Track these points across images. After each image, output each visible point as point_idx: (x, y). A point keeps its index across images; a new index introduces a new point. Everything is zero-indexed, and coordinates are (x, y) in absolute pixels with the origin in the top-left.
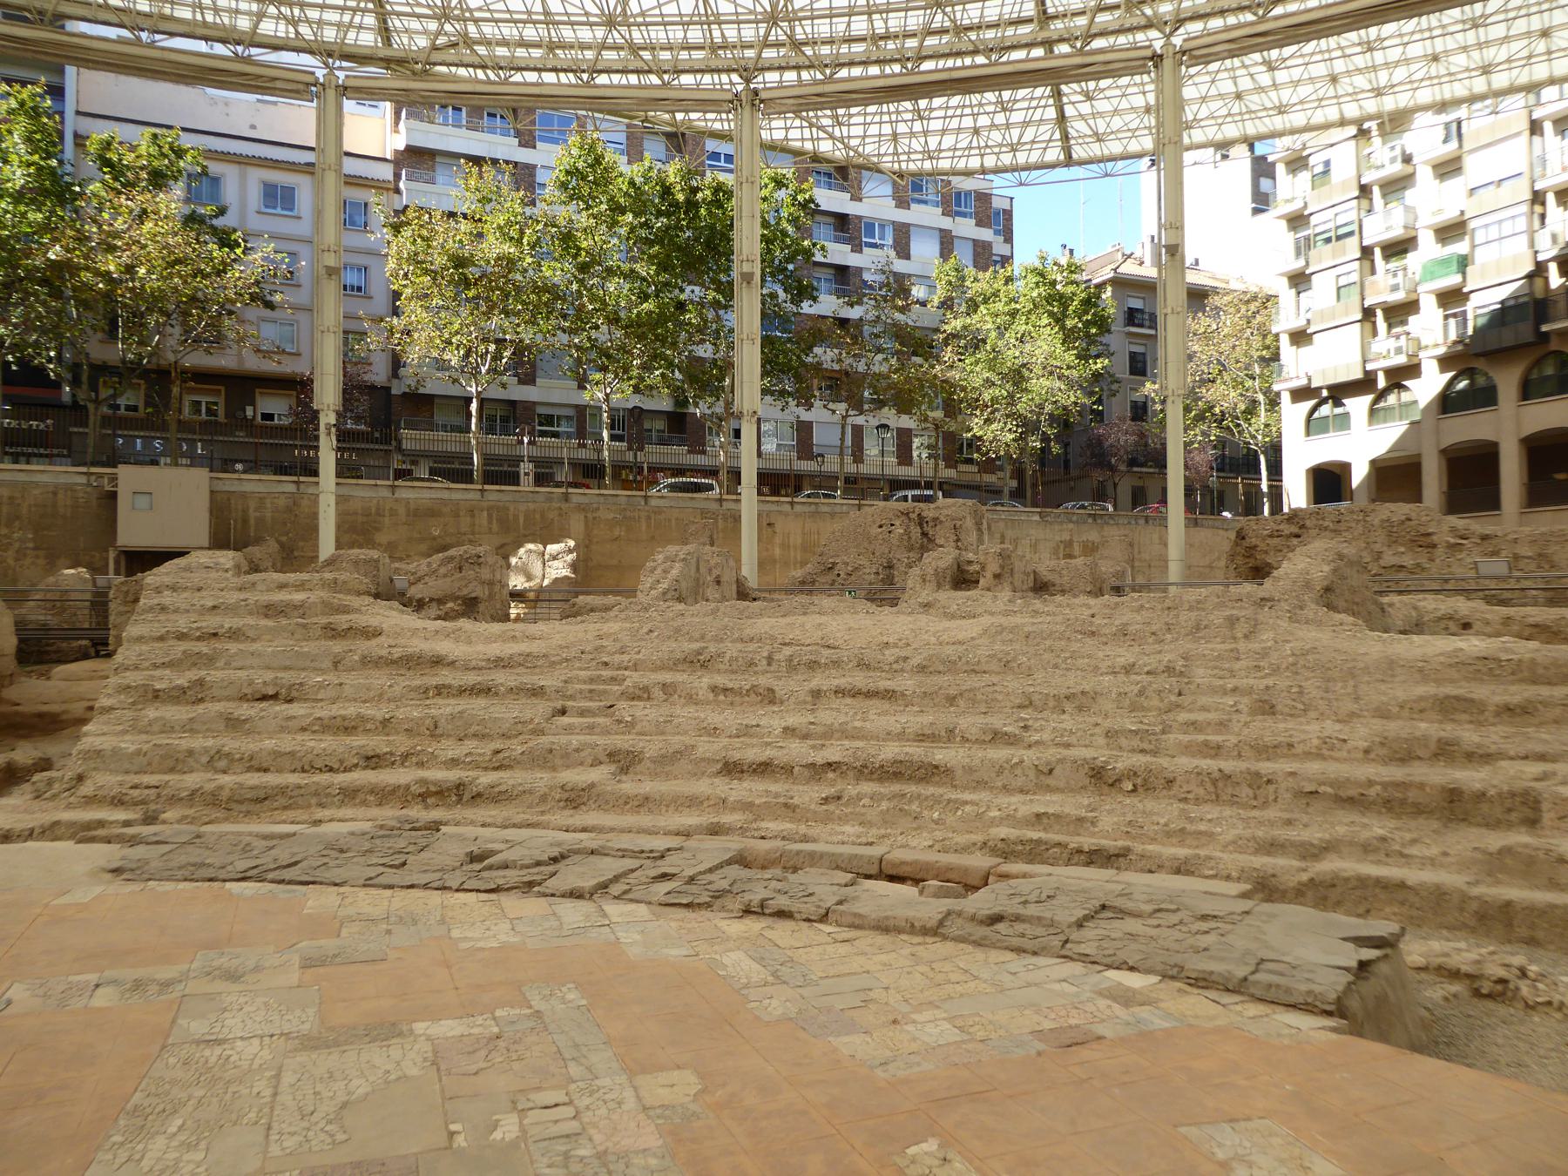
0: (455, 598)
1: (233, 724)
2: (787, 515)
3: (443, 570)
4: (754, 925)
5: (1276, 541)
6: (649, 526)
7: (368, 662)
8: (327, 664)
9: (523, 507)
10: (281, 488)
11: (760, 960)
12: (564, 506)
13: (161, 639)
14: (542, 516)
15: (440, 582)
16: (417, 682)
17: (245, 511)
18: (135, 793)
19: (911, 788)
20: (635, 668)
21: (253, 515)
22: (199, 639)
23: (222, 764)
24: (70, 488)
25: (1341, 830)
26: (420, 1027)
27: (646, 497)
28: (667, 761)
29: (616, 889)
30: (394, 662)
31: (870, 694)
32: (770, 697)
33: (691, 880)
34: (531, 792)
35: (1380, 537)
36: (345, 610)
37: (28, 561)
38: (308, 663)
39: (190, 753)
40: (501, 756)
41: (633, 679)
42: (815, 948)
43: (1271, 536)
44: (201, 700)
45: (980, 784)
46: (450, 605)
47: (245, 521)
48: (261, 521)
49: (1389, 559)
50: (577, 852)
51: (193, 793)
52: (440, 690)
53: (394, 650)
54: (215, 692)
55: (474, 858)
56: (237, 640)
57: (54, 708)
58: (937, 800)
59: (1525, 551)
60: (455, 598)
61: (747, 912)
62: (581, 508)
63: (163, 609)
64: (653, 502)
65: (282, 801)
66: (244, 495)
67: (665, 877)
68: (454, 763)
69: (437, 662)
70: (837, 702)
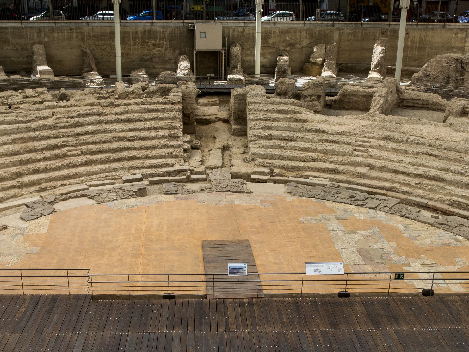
0: (315, 95)
1: (281, 147)
2: (414, 29)
3: (312, 87)
4: (402, 219)
6: (362, 34)
7: (308, 130)
8: (297, 130)
9: (318, 29)
10: (239, 25)
11: (404, 226)
12: (332, 28)
13: (257, 120)
14: (324, 32)
15: (311, 91)
16: (320, 138)
17: (229, 33)
18: (267, 164)
19: (436, 183)
20: (373, 138)
21: (231, 34)
22: (265, 120)
23: (282, 158)
24: (179, 27)
26: (359, 232)
27: (362, 24)
29: (378, 208)
30: (313, 131)
31: (431, 155)
32: (406, 152)
33: (391, 207)
34: (350, 172)
36: (298, 113)
37: (168, 51)
38: (293, 130)
39: (275, 155)
40: (343, 162)
42: (412, 224)
44: (271, 139)
46: (313, 97)
47: (229, 36)
48: (233, 36)
50: (369, 198)
51: (279, 166)
52: (326, 141)
53: (313, 127)
54: (274, 137)
55: (351, 197)
56: (274, 121)
57: (207, 117)
58: (441, 187)
60: (315, 95)
61: (401, 216)
62: (339, 29)
63: (255, 110)
64: (364, 26)
65: (297, 169)
66: (228, 28)
67: (386, 206)
68: (332, 162)
69: (323, 132)
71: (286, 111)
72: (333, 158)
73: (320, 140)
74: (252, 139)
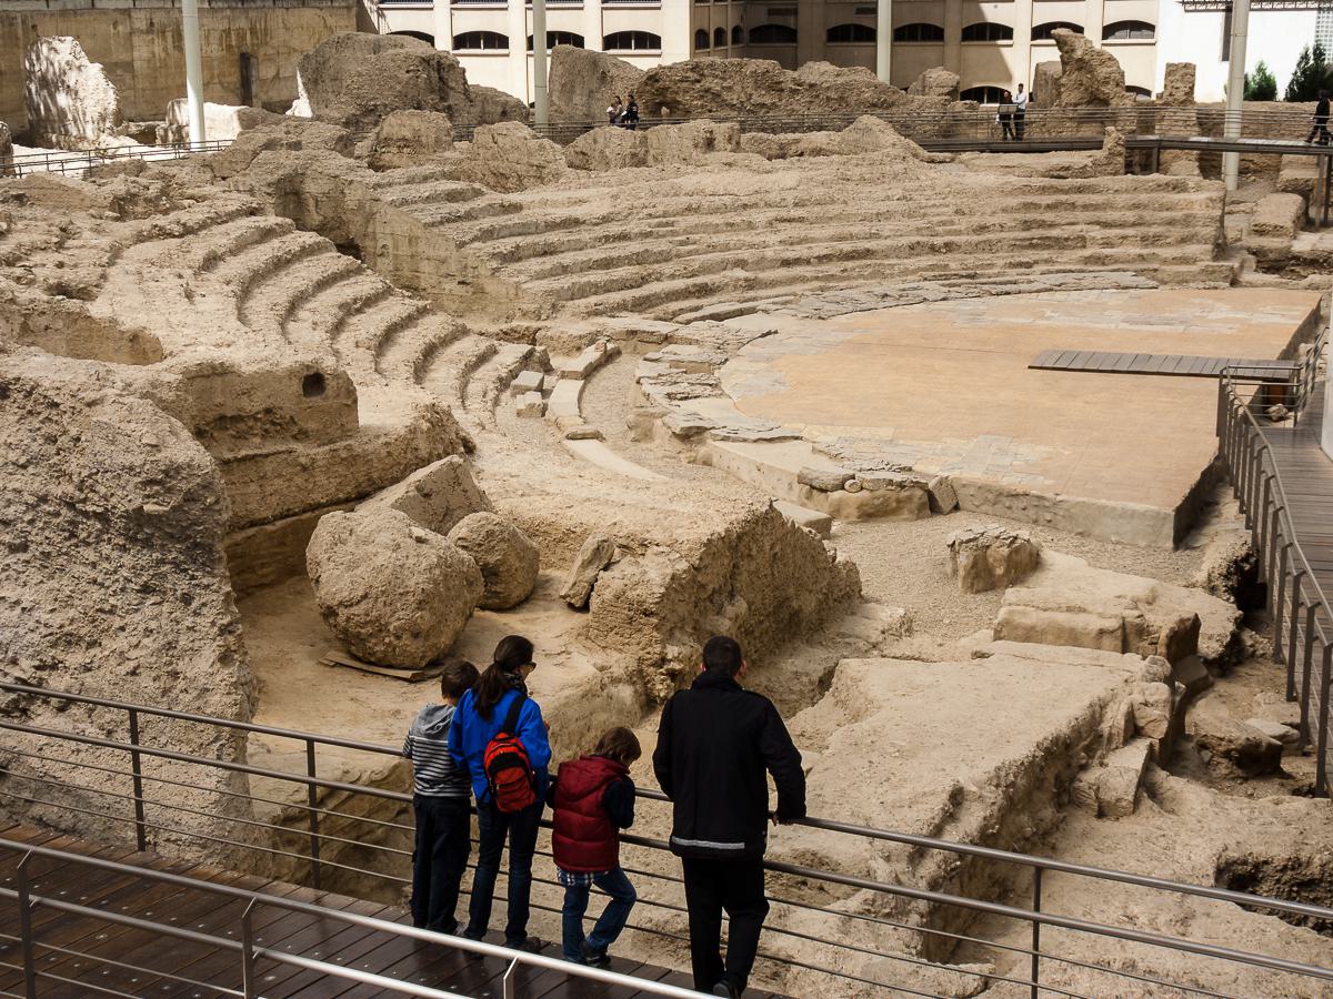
5: (685, 85)
8: (533, 229)
22: (454, 221)
25: (1036, 257)
28: (761, 263)
32: (751, 226)
35: (750, 83)
38: (526, 230)
41: (684, 222)
43: (682, 81)
44: (520, 259)
45: (887, 257)
49: (756, 99)
59: (833, 95)
68: (672, 277)
69: (577, 222)
70: (781, 226)
71: (460, 193)
72: (667, 268)
73: (595, 239)
74: (495, 264)
